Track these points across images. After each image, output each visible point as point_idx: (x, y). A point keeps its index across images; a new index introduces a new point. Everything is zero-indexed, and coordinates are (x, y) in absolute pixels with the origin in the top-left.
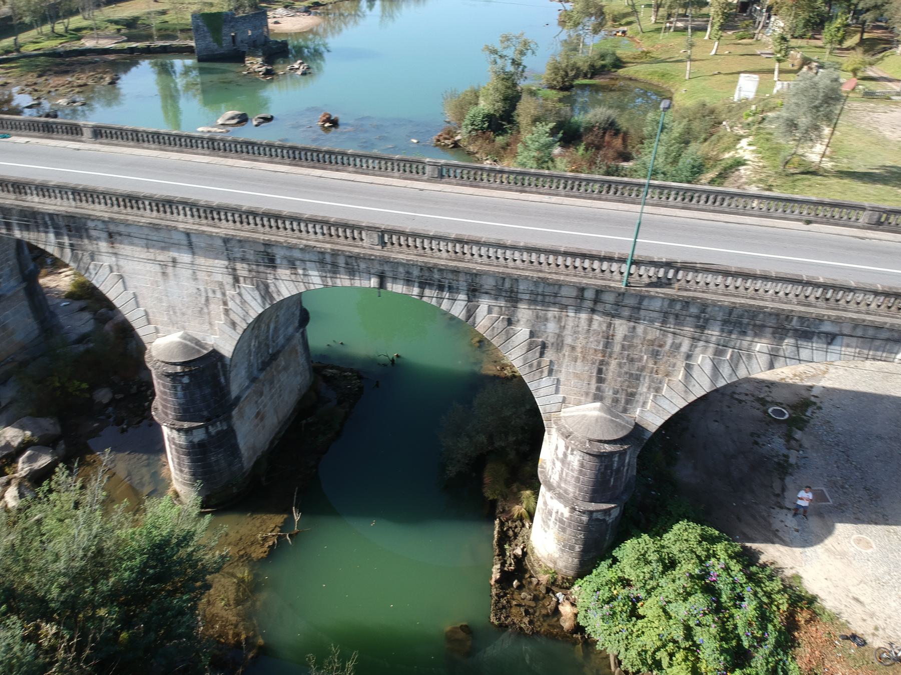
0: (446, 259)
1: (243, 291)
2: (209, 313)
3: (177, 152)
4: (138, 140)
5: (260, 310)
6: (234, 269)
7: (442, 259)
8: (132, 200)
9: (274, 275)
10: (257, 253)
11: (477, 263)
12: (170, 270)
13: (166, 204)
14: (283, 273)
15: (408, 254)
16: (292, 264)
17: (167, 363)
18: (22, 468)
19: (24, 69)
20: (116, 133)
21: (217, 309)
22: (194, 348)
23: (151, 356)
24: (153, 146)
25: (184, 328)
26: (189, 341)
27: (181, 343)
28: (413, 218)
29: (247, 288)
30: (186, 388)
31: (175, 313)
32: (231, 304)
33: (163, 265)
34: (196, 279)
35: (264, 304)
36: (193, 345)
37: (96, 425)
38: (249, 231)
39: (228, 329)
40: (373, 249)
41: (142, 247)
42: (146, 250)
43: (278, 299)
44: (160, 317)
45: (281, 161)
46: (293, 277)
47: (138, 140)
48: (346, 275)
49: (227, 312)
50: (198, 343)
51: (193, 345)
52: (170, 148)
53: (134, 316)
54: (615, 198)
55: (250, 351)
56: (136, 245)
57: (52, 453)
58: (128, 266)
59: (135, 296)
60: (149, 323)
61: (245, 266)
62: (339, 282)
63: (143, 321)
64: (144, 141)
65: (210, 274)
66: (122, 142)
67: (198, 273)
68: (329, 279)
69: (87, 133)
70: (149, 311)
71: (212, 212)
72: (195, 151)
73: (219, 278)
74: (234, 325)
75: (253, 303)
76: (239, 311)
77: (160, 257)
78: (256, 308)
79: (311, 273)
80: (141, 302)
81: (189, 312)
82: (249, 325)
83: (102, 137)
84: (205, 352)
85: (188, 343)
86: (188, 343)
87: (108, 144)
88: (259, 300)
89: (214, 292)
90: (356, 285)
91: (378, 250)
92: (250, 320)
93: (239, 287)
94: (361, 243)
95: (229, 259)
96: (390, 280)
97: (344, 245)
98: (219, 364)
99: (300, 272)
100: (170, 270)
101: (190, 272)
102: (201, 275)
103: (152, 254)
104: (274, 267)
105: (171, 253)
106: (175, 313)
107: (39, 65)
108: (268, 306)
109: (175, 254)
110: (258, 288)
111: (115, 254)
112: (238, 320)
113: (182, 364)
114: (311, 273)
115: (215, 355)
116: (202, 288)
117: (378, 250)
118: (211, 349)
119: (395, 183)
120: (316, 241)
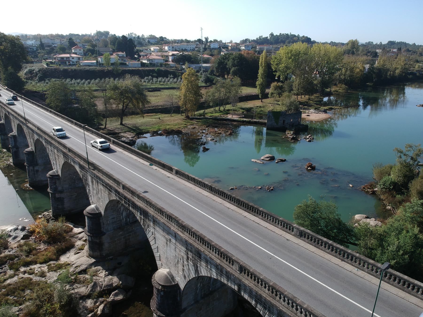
0: (267, 294)
1: (189, 264)
2: (178, 267)
3: (199, 187)
4: (188, 179)
5: (194, 276)
6: (188, 254)
7: (265, 293)
8: (161, 211)
9: (200, 263)
10: (196, 251)
11: (281, 304)
12: (168, 243)
13: (170, 217)
14: (203, 264)
15: (250, 282)
16: (207, 262)
17: (158, 283)
18: (111, 298)
19: (203, 123)
20: (182, 174)
21: (180, 267)
22: (170, 280)
23: (155, 276)
24: (192, 183)
25: (170, 269)
26: (170, 276)
27: (166, 275)
28: (271, 257)
29: (191, 263)
30: (162, 297)
31: (168, 261)
32: (185, 268)
33: (167, 240)
34: (176, 251)
35: (196, 274)
36: (170, 278)
37: (146, 288)
38: (193, 241)
39: (183, 278)
40: (236, 272)
41: (162, 230)
42: (162, 232)
43: (201, 275)
44: (164, 260)
45: (234, 203)
46: (206, 268)
47: (188, 179)
48: (226, 278)
49: (183, 270)
50: (173, 278)
51: (170, 278)
52: (197, 185)
53: (156, 255)
54: (397, 285)
55: (197, 289)
56: (160, 228)
57: (124, 295)
58: (158, 235)
59: (158, 248)
60: (160, 261)
61: (191, 254)
62: (222, 280)
63: (159, 259)
64: (190, 180)
65: (180, 251)
66: (183, 178)
67: (177, 249)
68: (219, 276)
69: (174, 171)
70: (161, 255)
71: (184, 228)
72: (205, 189)
73: (183, 254)
74: (185, 277)
75: (192, 271)
76: (187, 272)
77: (167, 236)
78: (193, 275)
79: (213, 270)
80: (159, 251)
81: (172, 263)
82: (190, 280)
83: (178, 174)
84: (173, 284)
85: (169, 276)
86: (169, 276)
87: (179, 177)
88: (194, 271)
89: (180, 259)
90: (229, 285)
91: (238, 273)
92: (190, 279)
93: (188, 262)
94: (232, 266)
95: (186, 249)
96: (243, 290)
97: (225, 264)
98: (178, 291)
99: (209, 267)
100: (168, 243)
101: (174, 247)
102: (177, 250)
103: (164, 234)
104: (201, 261)
105: (169, 237)
106: (168, 261)
107: (209, 122)
108: (197, 276)
109: (171, 238)
110: (194, 265)
111: (154, 228)
112: (187, 276)
113: (162, 286)
114: (213, 270)
115: (177, 286)
116: (177, 255)
117: (238, 273)
118: (176, 283)
119: (278, 231)
120: (215, 257)
